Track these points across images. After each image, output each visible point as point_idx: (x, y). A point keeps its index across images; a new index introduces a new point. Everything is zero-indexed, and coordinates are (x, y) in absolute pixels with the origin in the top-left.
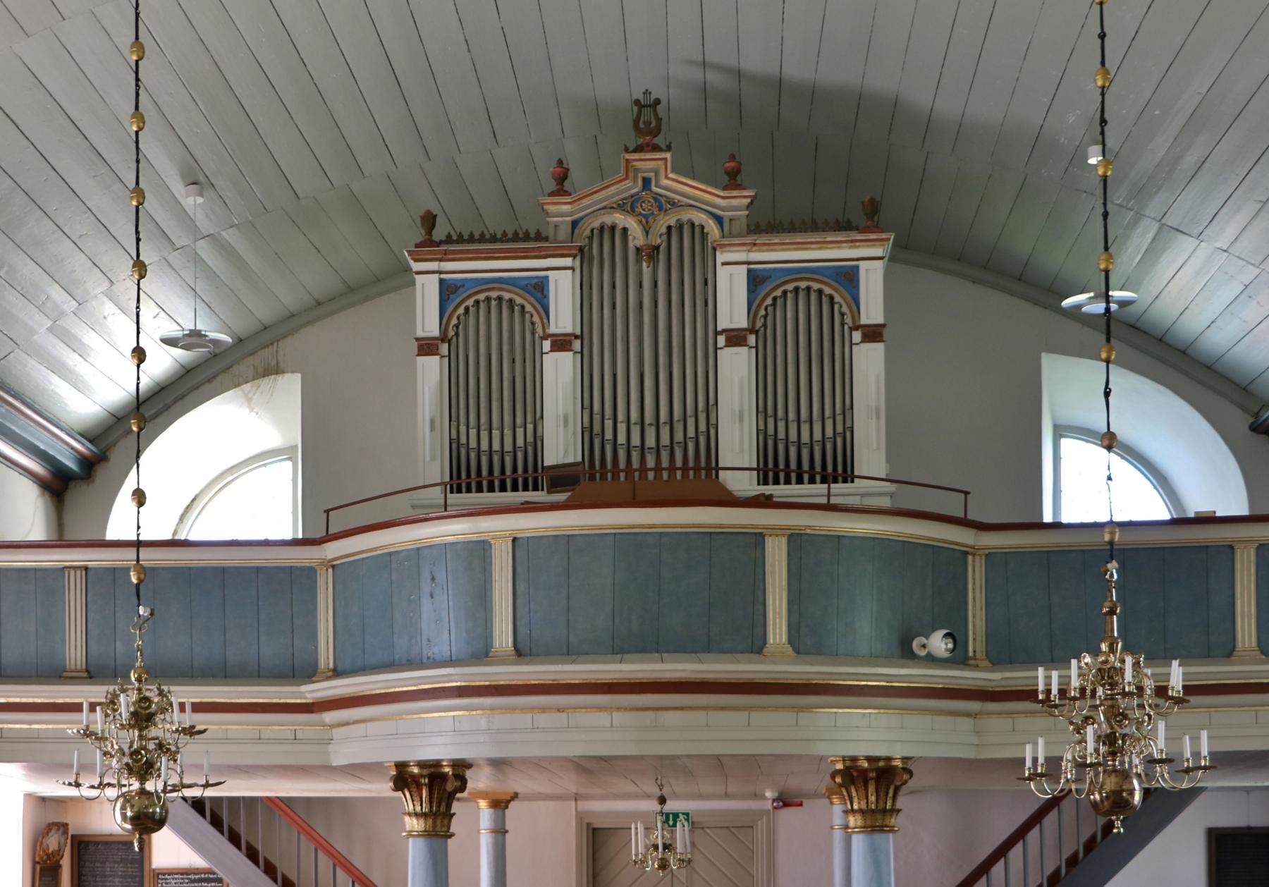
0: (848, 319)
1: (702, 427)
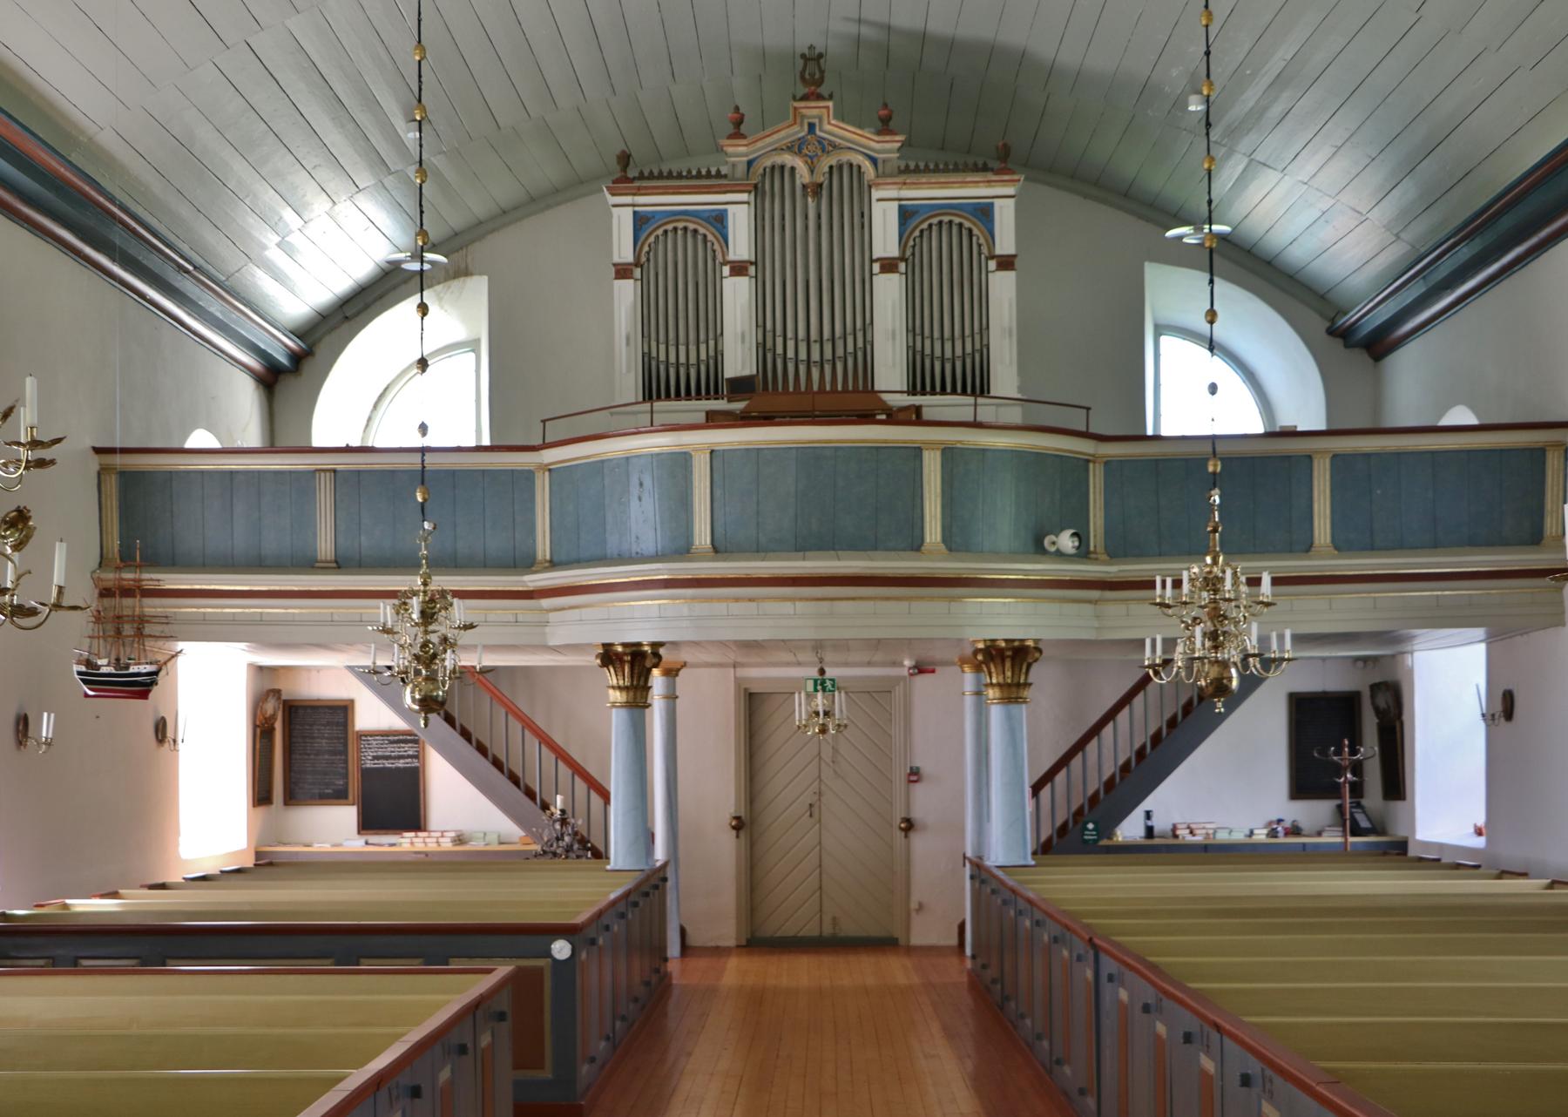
1: (860, 344)
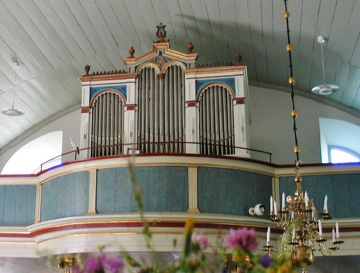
0: (232, 97)
